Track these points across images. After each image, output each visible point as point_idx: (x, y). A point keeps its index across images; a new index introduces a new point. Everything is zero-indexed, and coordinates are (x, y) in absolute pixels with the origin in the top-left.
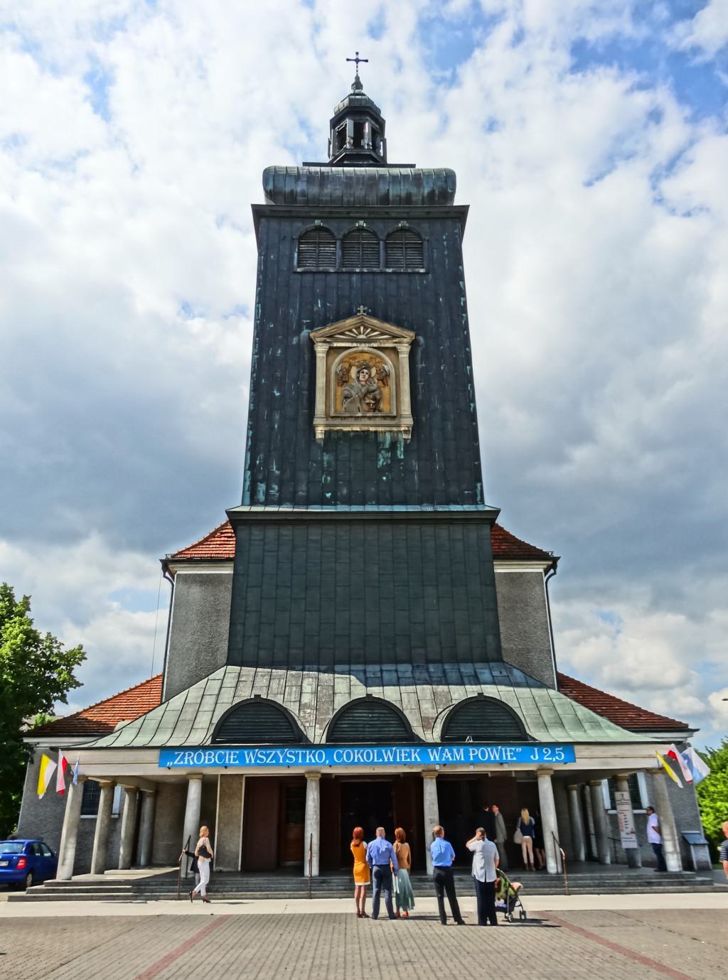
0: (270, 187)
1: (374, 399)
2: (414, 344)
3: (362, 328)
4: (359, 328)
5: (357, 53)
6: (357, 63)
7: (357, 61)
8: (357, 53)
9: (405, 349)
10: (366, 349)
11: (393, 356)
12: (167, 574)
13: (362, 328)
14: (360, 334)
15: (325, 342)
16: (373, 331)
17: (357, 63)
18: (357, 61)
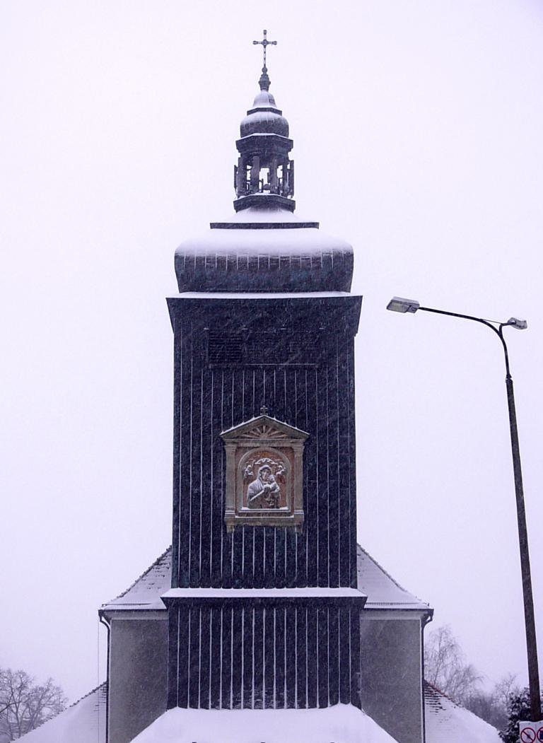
0: (182, 272)
1: (273, 497)
2: (308, 443)
3: (264, 427)
4: (262, 427)
5: (265, 33)
6: (265, 47)
7: (265, 43)
8: (265, 33)
9: (299, 448)
10: (267, 449)
11: (290, 455)
12: (103, 619)
13: (264, 427)
14: (262, 432)
15: (234, 443)
16: (274, 430)
17: (265, 47)
18: (265, 43)
